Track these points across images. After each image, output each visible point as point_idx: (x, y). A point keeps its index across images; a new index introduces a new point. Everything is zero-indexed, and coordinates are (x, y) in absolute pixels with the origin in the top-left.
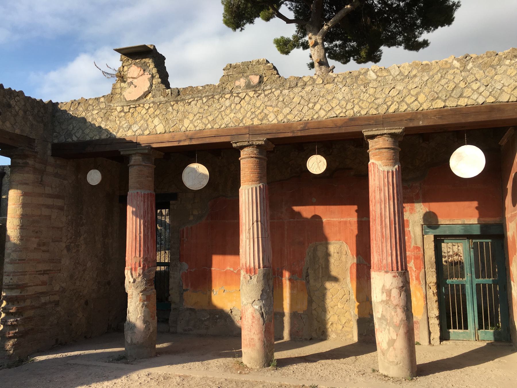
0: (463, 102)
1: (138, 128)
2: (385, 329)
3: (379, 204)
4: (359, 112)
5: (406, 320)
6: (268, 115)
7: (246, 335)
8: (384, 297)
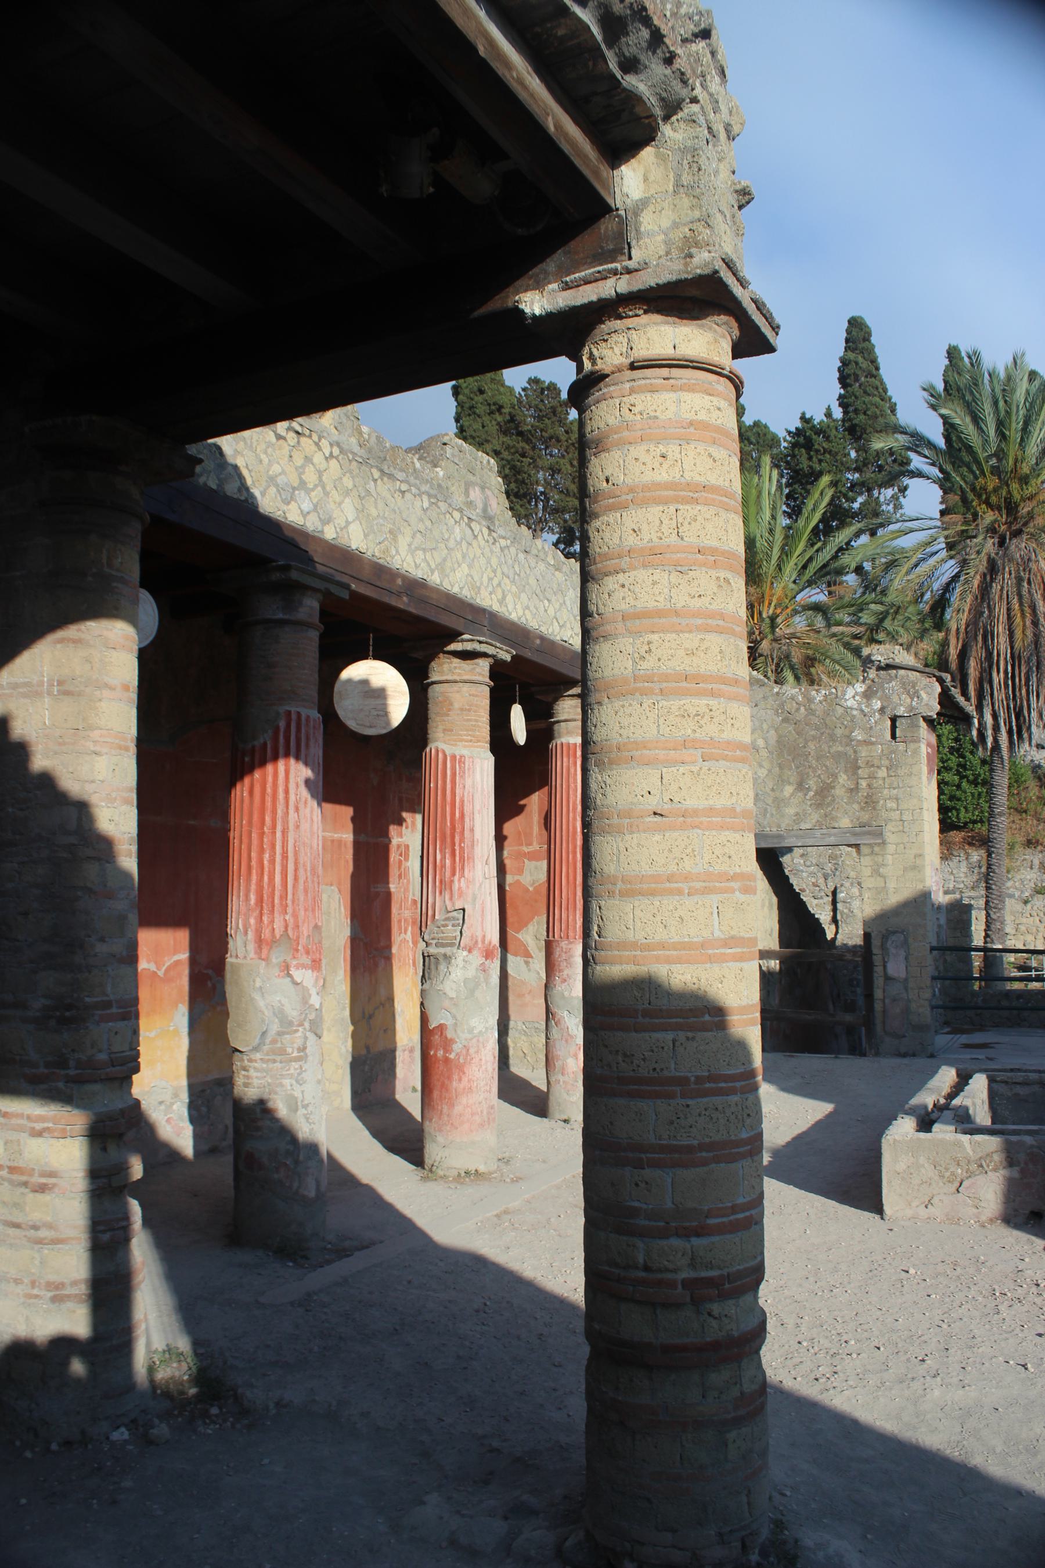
7: (480, 1103)
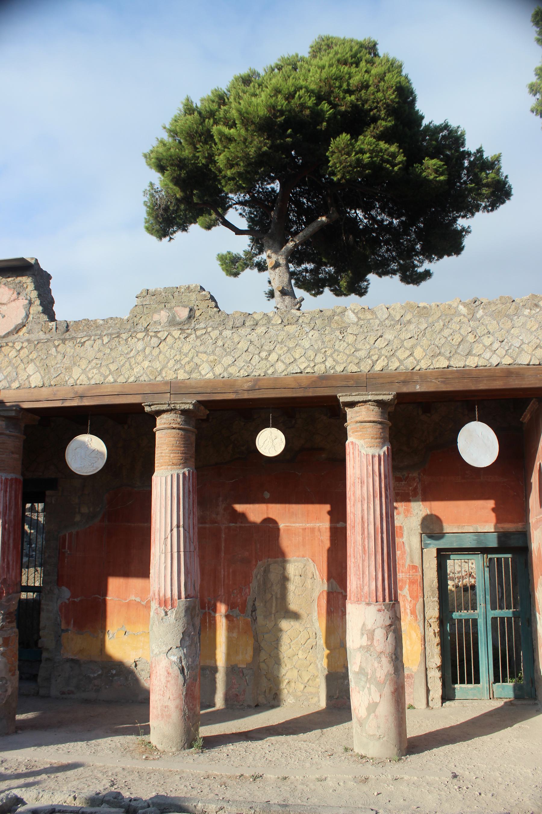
0: (472, 362)
1: (3, 377)
2: (364, 688)
3: (360, 503)
4: (334, 368)
5: (394, 673)
6: (200, 366)
7: (156, 701)
8: (364, 641)
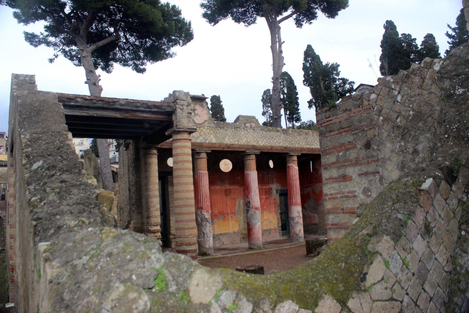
0: (313, 147)
